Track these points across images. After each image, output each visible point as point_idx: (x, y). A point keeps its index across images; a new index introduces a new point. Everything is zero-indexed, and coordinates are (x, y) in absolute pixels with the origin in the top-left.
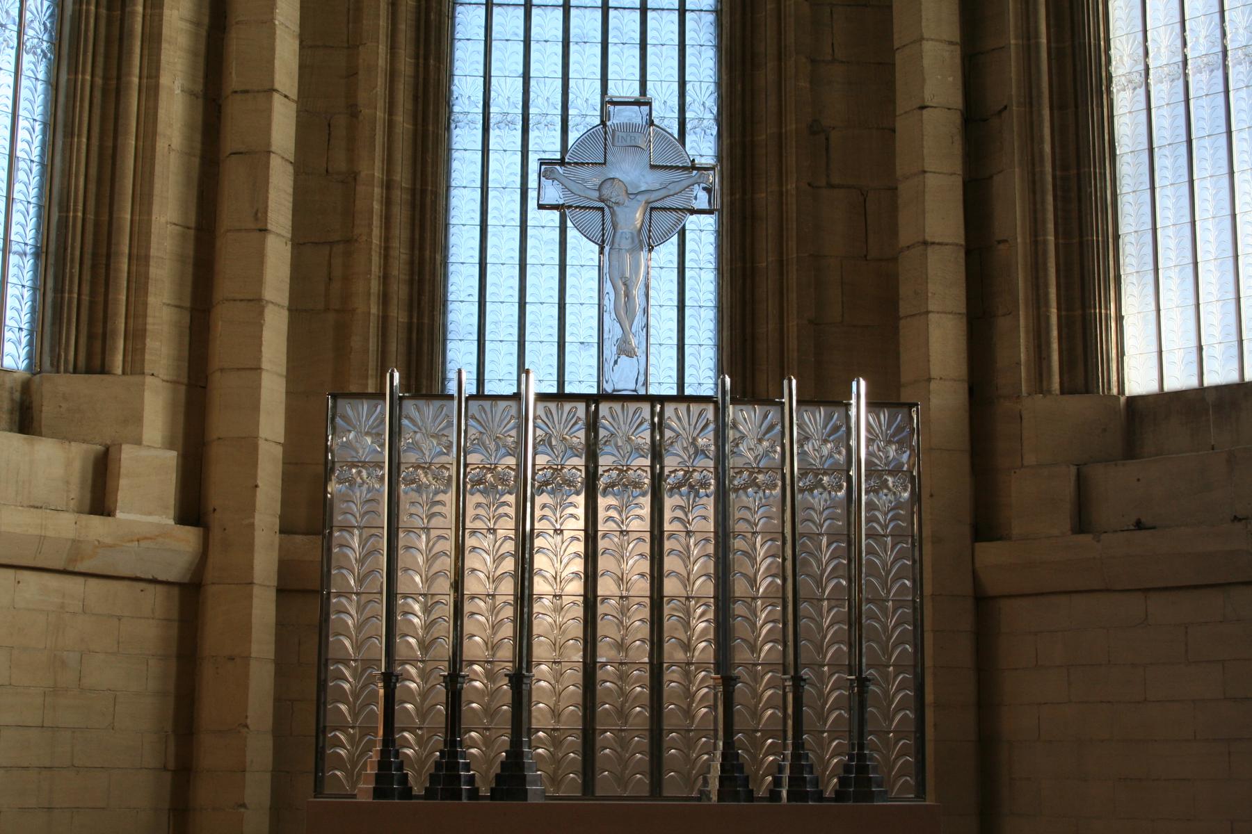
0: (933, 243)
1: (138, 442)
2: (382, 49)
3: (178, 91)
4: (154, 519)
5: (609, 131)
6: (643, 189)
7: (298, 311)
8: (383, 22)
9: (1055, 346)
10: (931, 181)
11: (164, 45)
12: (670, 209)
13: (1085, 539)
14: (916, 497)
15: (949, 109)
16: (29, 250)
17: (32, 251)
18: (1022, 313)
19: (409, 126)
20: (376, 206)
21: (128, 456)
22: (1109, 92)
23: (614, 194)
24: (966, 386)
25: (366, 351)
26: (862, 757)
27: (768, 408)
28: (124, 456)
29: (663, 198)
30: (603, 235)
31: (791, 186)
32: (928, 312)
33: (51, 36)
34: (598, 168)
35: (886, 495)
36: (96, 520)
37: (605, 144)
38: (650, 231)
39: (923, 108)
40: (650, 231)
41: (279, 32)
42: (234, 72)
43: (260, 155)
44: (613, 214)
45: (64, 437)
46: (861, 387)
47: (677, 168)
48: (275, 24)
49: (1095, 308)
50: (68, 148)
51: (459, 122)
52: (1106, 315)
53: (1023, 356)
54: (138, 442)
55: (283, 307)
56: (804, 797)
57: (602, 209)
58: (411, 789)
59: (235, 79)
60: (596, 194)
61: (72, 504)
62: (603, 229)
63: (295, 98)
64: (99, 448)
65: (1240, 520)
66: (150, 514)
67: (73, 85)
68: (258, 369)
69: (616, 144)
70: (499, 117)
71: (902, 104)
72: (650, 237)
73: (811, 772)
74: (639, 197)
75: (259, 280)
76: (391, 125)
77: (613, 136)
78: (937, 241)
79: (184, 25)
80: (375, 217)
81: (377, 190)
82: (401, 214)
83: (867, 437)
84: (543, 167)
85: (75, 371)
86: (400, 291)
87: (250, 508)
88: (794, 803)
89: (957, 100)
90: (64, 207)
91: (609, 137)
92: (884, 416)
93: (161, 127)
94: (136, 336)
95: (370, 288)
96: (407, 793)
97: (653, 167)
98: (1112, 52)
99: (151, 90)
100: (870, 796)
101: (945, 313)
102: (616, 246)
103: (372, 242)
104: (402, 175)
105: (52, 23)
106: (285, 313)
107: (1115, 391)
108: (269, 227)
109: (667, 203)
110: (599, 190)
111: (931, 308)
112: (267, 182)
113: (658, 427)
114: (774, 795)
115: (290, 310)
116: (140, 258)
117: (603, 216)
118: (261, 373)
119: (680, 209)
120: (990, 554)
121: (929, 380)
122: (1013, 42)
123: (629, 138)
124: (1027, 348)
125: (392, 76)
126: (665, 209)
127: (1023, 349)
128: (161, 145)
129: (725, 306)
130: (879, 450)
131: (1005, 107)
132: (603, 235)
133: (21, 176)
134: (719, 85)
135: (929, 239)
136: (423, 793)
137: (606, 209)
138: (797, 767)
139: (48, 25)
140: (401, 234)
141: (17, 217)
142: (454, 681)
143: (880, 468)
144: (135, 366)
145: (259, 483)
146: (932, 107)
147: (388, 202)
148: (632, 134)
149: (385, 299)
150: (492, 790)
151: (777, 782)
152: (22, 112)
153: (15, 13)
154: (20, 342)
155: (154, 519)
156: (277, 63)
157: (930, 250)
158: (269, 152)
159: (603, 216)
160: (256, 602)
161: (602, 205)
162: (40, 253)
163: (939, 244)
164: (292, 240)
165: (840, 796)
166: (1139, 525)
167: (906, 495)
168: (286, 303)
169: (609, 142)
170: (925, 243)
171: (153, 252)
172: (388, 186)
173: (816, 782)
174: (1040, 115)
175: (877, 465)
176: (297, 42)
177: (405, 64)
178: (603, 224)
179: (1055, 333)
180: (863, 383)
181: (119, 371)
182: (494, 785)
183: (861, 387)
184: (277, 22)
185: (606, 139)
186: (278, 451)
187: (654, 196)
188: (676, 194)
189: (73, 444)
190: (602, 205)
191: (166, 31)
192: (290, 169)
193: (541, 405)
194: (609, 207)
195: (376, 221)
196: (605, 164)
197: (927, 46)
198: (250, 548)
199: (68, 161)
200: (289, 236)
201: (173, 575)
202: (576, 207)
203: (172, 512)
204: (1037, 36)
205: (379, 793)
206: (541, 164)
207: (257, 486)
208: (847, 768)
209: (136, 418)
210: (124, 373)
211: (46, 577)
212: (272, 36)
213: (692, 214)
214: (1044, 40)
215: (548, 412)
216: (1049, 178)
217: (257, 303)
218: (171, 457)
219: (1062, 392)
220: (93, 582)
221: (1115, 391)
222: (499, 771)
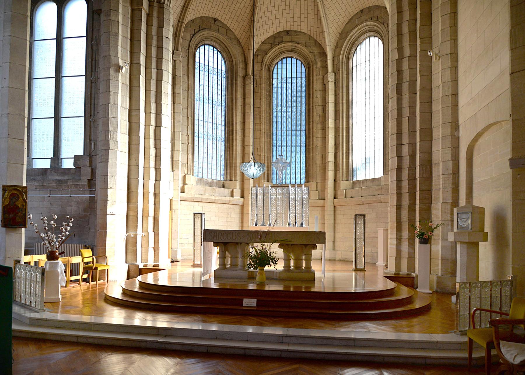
1: (236, 189)
2: (263, 138)
19: (267, 148)
50: (227, 154)
59: (246, 144)
67: (227, 146)
71: (327, 144)
82: (266, 159)
89: (333, 143)
90: (227, 161)
93: (238, 151)
94: (236, 176)
104: (266, 154)
128: (238, 153)
133: (222, 157)
141: (222, 162)
144: (235, 180)
152: (222, 150)
153: (220, 137)
166: (351, 197)
177: (266, 140)
191: (238, 139)
199: (227, 155)
211: (226, 205)
212: (250, 138)
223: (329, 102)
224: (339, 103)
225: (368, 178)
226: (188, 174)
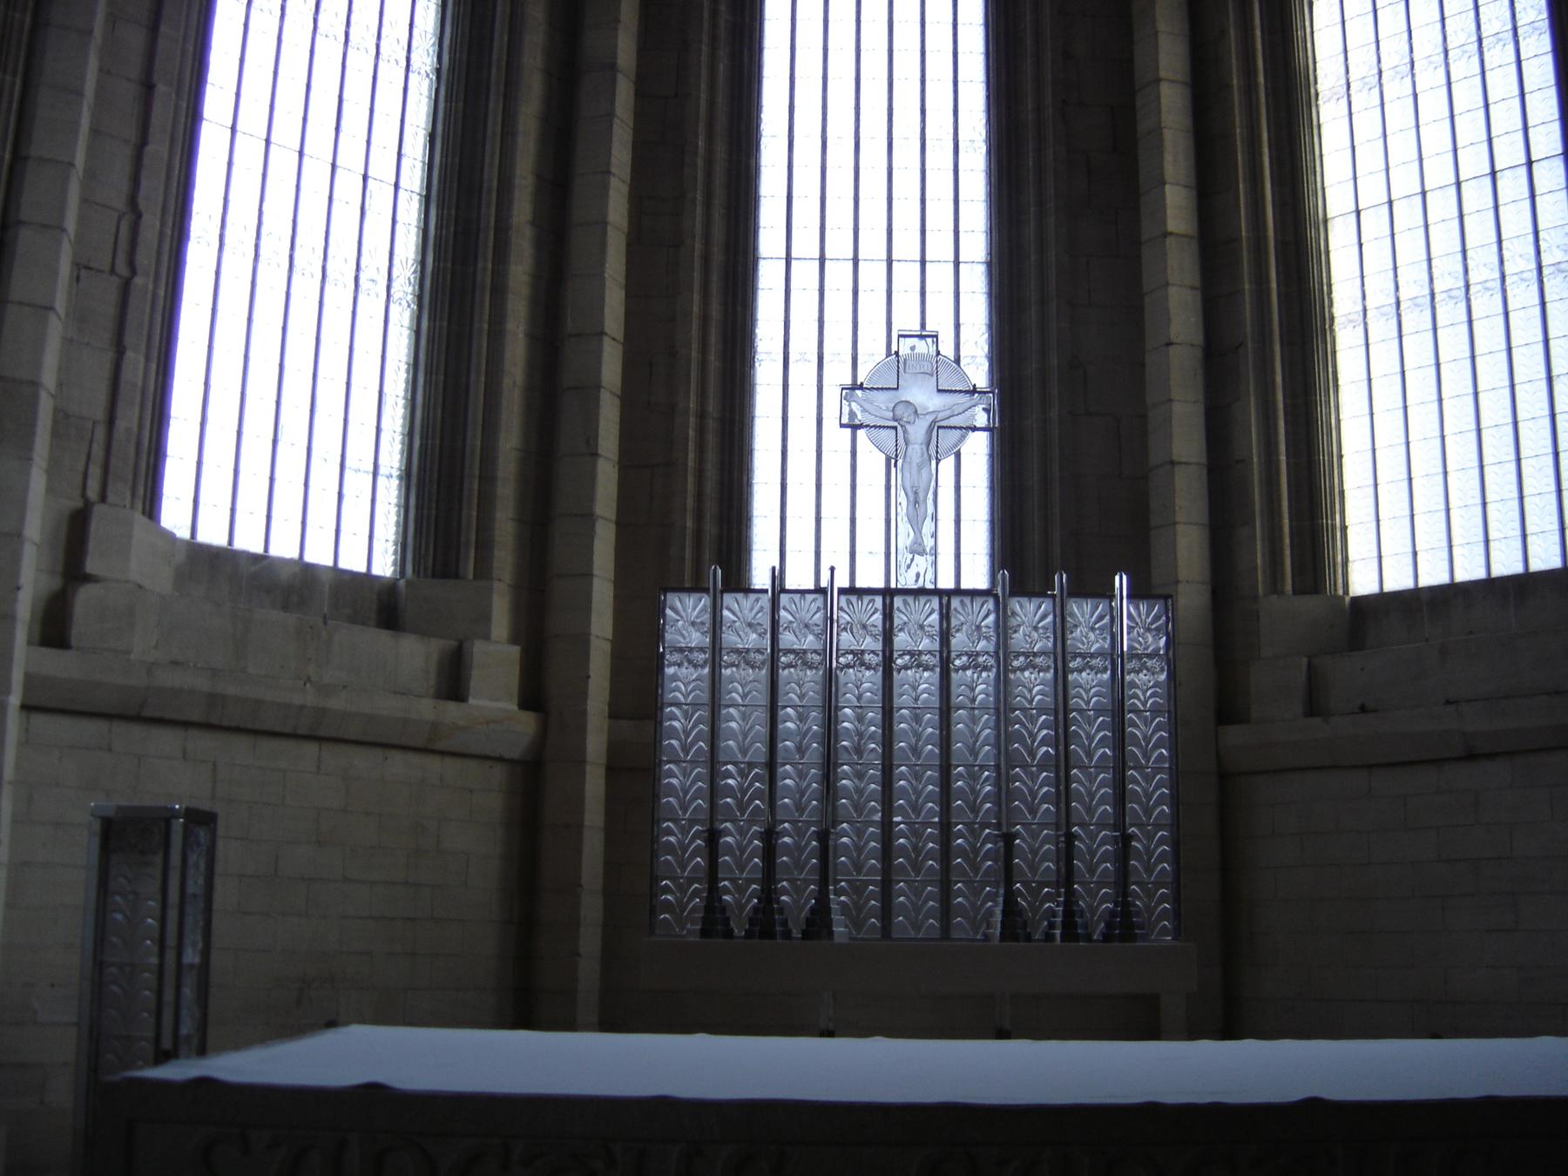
0: (1180, 463)
1: (486, 637)
2: (696, 297)
3: (521, 336)
4: (502, 705)
5: (901, 360)
6: (931, 410)
7: (624, 526)
8: (697, 275)
9: (1288, 552)
10: (1178, 409)
11: (510, 296)
12: (955, 428)
13: (1316, 721)
14: (1172, 676)
15: (1192, 345)
16: (396, 473)
17: (398, 473)
18: (1258, 523)
20: (691, 433)
21: (479, 649)
22: (1332, 331)
23: (906, 415)
24: (1209, 587)
25: (683, 559)
26: (1126, 905)
27: (1042, 600)
28: (475, 650)
29: (949, 418)
30: (897, 450)
31: (1054, 414)
32: (1175, 523)
33: (414, 290)
34: (894, 392)
35: (1145, 675)
36: (452, 707)
37: (898, 371)
38: (937, 447)
39: (1169, 344)
40: (937, 447)
41: (609, 284)
42: (569, 319)
43: (592, 388)
44: (905, 432)
45: (424, 633)
46: (1121, 582)
47: (961, 391)
48: (604, 277)
49: (1322, 519)
51: (762, 360)
52: (1332, 524)
53: (1259, 561)
54: (486, 637)
55: (610, 521)
56: (1076, 938)
57: (895, 428)
58: (732, 930)
60: (891, 414)
61: (432, 691)
62: (896, 445)
63: (622, 341)
64: (454, 643)
65: (1451, 703)
66: (497, 700)
68: (589, 575)
69: (907, 370)
70: (799, 357)
72: (937, 452)
73: (1082, 917)
74: (927, 417)
75: (591, 498)
76: (703, 363)
77: (905, 364)
78: (1183, 460)
79: (525, 278)
80: (690, 443)
81: (692, 420)
82: (712, 440)
83: (1128, 625)
84: (844, 392)
85: (434, 576)
86: (711, 508)
87: (583, 695)
88: (1066, 944)
89: (1199, 338)
91: (901, 365)
92: (1143, 608)
94: (485, 547)
95: (685, 504)
96: (729, 934)
97: (939, 391)
98: (1334, 295)
99: (497, 335)
100: (1132, 938)
101: (1190, 523)
102: (908, 459)
103: (687, 465)
104: (713, 407)
105: (415, 278)
106: (613, 527)
107: (1340, 592)
108: (600, 452)
109: (953, 422)
110: (893, 410)
111: (1178, 519)
112: (597, 414)
113: (945, 615)
114: (1049, 937)
115: (617, 524)
116: (488, 478)
117: (897, 434)
118: (592, 580)
119: (963, 428)
120: (1234, 735)
121: (1177, 582)
122: (1247, 286)
123: (918, 366)
124: (1263, 555)
125: (705, 319)
126: (951, 428)
127: (1259, 555)
128: (507, 381)
129: (996, 521)
130: (1139, 635)
131: (1241, 344)
132: (897, 450)
134: (990, 327)
135: (1175, 458)
136: (743, 933)
137: (899, 428)
138: (1069, 914)
139: (412, 280)
140: (712, 457)
142: (770, 837)
143: (1140, 652)
144: (484, 571)
145: (591, 674)
146: (1177, 344)
147: (701, 430)
148: (921, 363)
149: (699, 516)
150: (804, 932)
151: (1051, 926)
154: (386, 552)
155: (502, 705)
156: (607, 310)
157: (1177, 468)
158: (598, 387)
159: (897, 434)
160: (588, 777)
161: (895, 424)
162: (406, 476)
163: (1185, 463)
164: (620, 462)
165: (1107, 938)
166: (1363, 709)
167: (1163, 677)
168: (614, 517)
169: (901, 370)
170: (1172, 463)
171: (500, 474)
172: (702, 415)
173: (1086, 927)
174: (1272, 351)
175: (1137, 649)
176: (623, 292)
177: (715, 310)
178: (897, 441)
179: (1287, 541)
180: (1125, 577)
181: (471, 576)
182: (804, 927)
183: (1121, 582)
184: (606, 275)
185: (898, 367)
186: (607, 647)
187: (941, 416)
188: (960, 414)
189: (432, 639)
190: (895, 424)
192: (617, 402)
193: (843, 598)
194: (902, 426)
195: (691, 446)
196: (897, 389)
197: (1172, 291)
198: (582, 730)
200: (617, 459)
201: (516, 753)
202: (872, 427)
203: (516, 700)
204: (1268, 281)
205: (705, 933)
206: (843, 389)
207: (589, 677)
208: (1112, 913)
209: (485, 617)
210: (475, 577)
213: (973, 431)
214: (1274, 285)
215: (849, 602)
216: (1281, 406)
217: (589, 518)
218: (515, 651)
219: (1295, 592)
220: (448, 761)
221: (1340, 592)
222: (808, 915)
223: (1158, 80)
224: (1228, 86)
225: (1469, 569)
226: (111, 497)
